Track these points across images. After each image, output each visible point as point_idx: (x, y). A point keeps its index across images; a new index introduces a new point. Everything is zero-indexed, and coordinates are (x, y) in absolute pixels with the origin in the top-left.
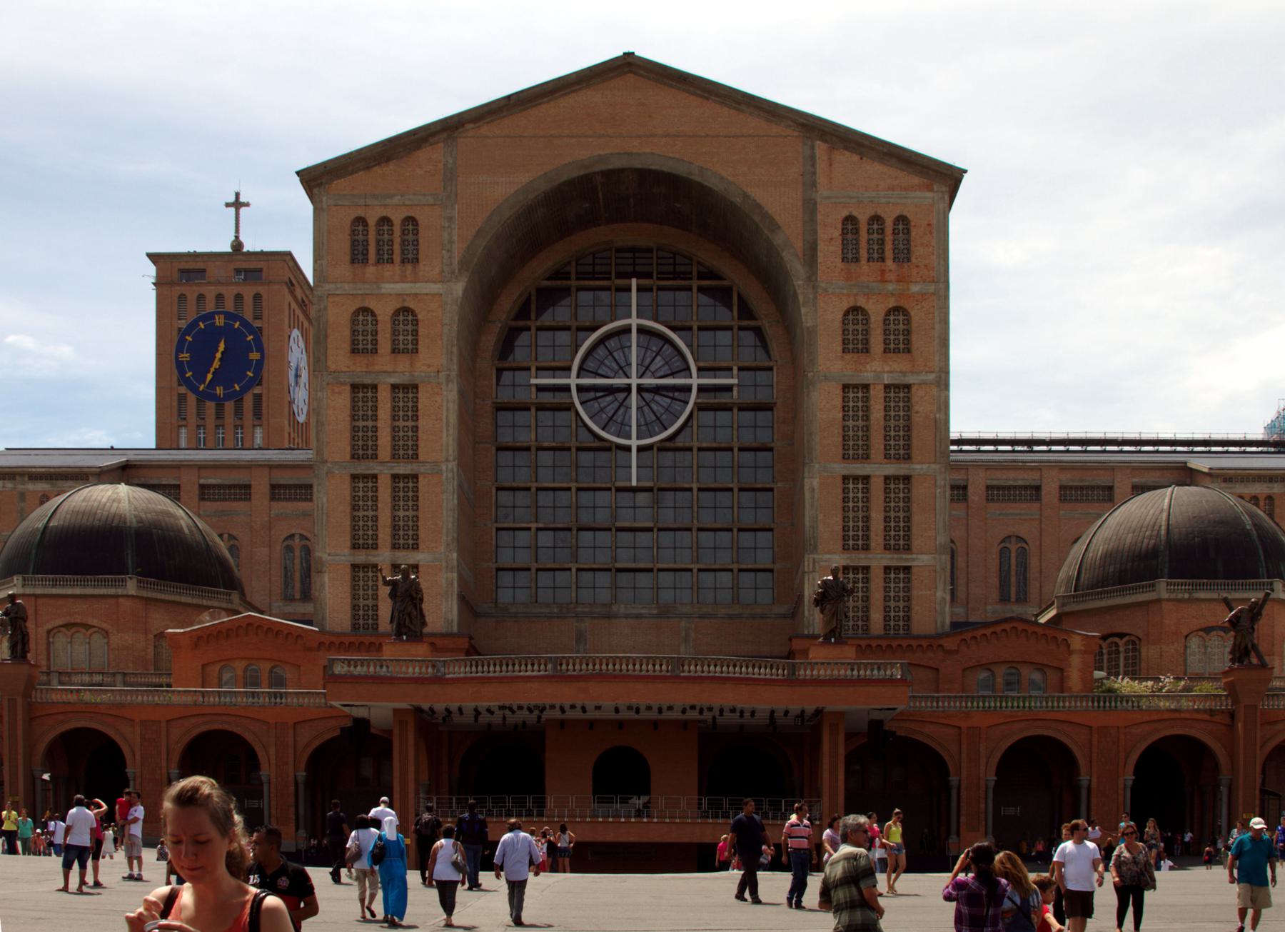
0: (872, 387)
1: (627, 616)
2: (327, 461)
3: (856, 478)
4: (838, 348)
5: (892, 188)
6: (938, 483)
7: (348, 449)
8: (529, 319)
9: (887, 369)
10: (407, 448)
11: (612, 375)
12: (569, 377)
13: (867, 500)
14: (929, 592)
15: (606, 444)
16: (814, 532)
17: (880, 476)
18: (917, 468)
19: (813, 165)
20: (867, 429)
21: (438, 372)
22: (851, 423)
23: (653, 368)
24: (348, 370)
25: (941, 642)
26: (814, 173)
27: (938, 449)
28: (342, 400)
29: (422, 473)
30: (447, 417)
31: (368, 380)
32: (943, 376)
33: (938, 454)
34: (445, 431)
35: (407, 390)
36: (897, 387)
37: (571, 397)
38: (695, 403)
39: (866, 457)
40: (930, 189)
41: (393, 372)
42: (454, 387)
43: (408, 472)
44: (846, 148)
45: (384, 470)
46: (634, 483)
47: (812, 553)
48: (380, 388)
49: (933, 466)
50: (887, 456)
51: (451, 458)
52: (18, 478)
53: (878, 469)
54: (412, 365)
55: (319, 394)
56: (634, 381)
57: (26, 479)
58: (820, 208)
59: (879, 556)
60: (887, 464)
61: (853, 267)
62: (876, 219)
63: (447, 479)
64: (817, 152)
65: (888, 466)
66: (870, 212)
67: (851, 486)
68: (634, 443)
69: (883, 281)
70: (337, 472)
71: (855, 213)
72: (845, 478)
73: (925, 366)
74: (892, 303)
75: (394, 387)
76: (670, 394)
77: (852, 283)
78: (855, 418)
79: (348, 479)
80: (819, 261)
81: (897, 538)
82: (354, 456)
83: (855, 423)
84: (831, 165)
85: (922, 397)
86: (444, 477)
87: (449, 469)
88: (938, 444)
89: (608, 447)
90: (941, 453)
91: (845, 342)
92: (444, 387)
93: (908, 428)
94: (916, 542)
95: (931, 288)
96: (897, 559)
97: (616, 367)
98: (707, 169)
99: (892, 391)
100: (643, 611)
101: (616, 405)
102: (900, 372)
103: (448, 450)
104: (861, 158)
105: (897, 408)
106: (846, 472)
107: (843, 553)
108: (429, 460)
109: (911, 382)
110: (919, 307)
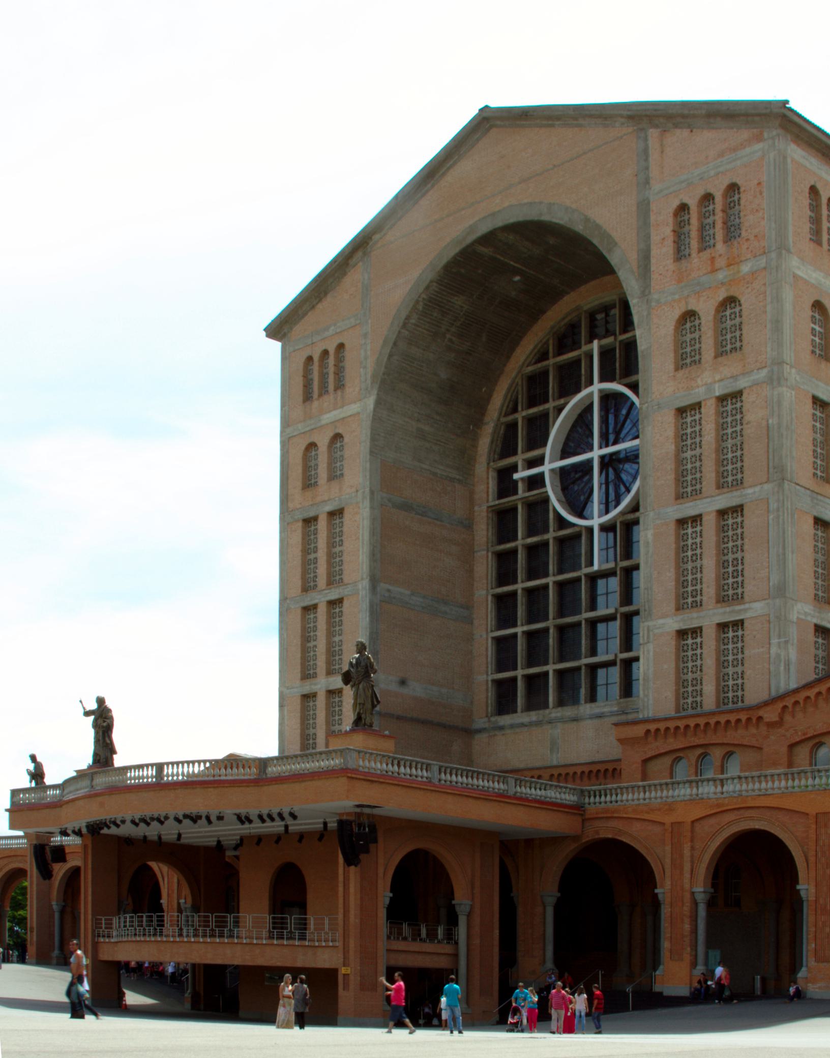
0: (703, 404)
5: (721, 155)
6: (771, 508)
9: (717, 377)
14: (762, 650)
16: (648, 594)
18: (749, 494)
19: (646, 160)
21: (357, 491)
24: (299, 506)
25: (761, 713)
26: (647, 168)
27: (771, 465)
33: (771, 470)
35: (336, 514)
40: (759, 138)
44: (676, 126)
45: (320, 598)
49: (766, 486)
50: (720, 486)
58: (653, 207)
59: (711, 612)
60: (719, 495)
61: (684, 263)
62: (708, 198)
64: (650, 143)
65: (720, 497)
66: (700, 192)
69: (714, 271)
70: (293, 607)
71: (686, 200)
73: (756, 361)
74: (722, 295)
77: (683, 284)
79: (299, 612)
80: (652, 269)
83: (693, 453)
84: (662, 152)
85: (754, 402)
86: (360, 596)
87: (364, 585)
88: (771, 457)
90: (774, 468)
92: (361, 505)
94: (749, 588)
95: (762, 262)
96: (730, 612)
98: (554, 204)
99: (729, 402)
100: (606, 710)
102: (731, 377)
104: (692, 131)
106: (680, 516)
107: (675, 615)
108: (351, 582)
110: (750, 290)
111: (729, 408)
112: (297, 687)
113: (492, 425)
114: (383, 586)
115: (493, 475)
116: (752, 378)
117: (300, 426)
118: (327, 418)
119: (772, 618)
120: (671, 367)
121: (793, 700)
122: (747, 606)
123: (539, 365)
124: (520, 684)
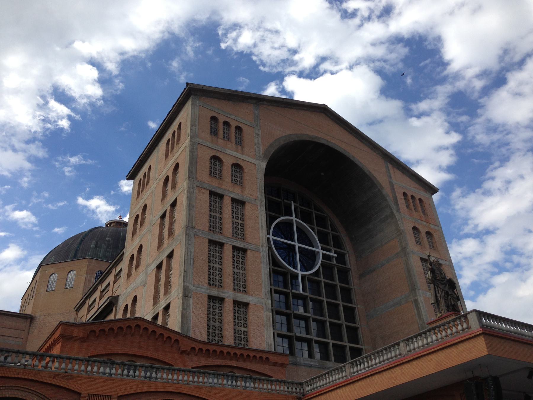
1: (305, 365)
24: (208, 183)
28: (205, 197)
29: (249, 249)
31: (219, 191)
35: (239, 203)
43: (242, 246)
46: (301, 292)
51: (265, 245)
54: (242, 192)
55: (192, 190)
63: (263, 256)
68: (300, 273)
75: (234, 200)
92: (259, 207)
100: (312, 363)
103: (263, 240)
109: (442, 263)
112: (204, 289)
117: (208, 143)
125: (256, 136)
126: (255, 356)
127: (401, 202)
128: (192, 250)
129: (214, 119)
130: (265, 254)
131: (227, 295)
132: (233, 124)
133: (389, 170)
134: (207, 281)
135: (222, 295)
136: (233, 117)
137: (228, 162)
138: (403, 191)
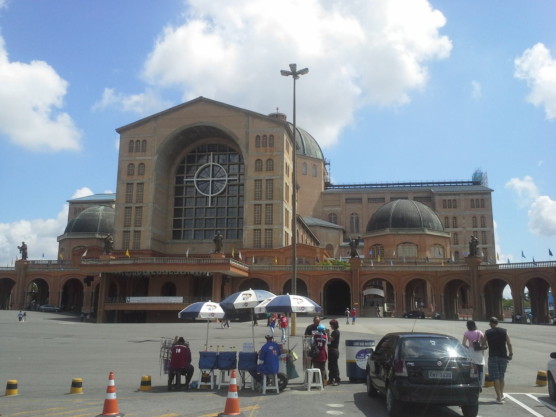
0: (262, 180)
1: (206, 243)
2: (119, 204)
3: (258, 205)
4: (254, 170)
7: (125, 200)
8: (184, 163)
9: (267, 175)
10: (140, 199)
11: (206, 177)
12: (194, 178)
13: (261, 210)
15: (204, 196)
17: (264, 204)
18: (274, 202)
20: (261, 191)
21: (149, 179)
22: (257, 190)
23: (217, 175)
24: (125, 179)
28: (124, 187)
30: (151, 191)
32: (282, 177)
34: (150, 195)
36: (270, 180)
37: (194, 184)
38: (227, 184)
39: (261, 199)
41: (138, 180)
42: (153, 183)
46: (210, 206)
47: (245, 225)
48: (134, 184)
49: (279, 201)
52: (90, 203)
53: (264, 202)
56: (211, 179)
57: (93, 203)
67: (257, 207)
72: (255, 205)
75: (138, 184)
76: (221, 182)
78: (259, 188)
81: (269, 221)
82: (127, 202)
89: (203, 197)
91: (256, 168)
93: (272, 191)
94: (274, 222)
97: (207, 175)
101: (207, 185)
105: (270, 186)
111: (268, 182)
113: (176, 165)
114: (155, 205)
115: (175, 178)
116: (275, 177)
118: (138, 158)
119: (280, 229)
120: (254, 170)
121: (287, 248)
122: (273, 226)
123: (193, 154)
124: (182, 232)
125: (154, 141)
126: (136, 253)
127: (252, 144)
128: (118, 214)
129: (132, 141)
130: (151, 207)
131: (131, 229)
132: (141, 141)
133: (249, 123)
134: (123, 225)
135: (129, 230)
136: (141, 136)
137: (136, 164)
138: (256, 135)
